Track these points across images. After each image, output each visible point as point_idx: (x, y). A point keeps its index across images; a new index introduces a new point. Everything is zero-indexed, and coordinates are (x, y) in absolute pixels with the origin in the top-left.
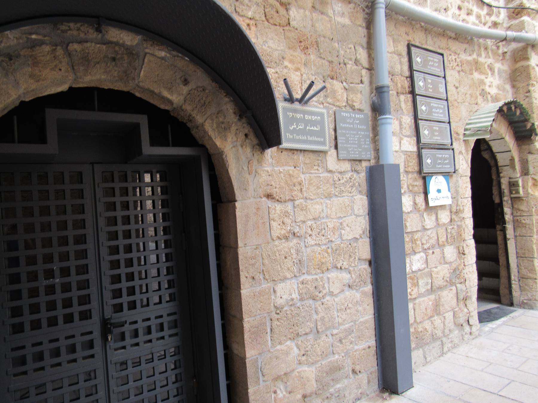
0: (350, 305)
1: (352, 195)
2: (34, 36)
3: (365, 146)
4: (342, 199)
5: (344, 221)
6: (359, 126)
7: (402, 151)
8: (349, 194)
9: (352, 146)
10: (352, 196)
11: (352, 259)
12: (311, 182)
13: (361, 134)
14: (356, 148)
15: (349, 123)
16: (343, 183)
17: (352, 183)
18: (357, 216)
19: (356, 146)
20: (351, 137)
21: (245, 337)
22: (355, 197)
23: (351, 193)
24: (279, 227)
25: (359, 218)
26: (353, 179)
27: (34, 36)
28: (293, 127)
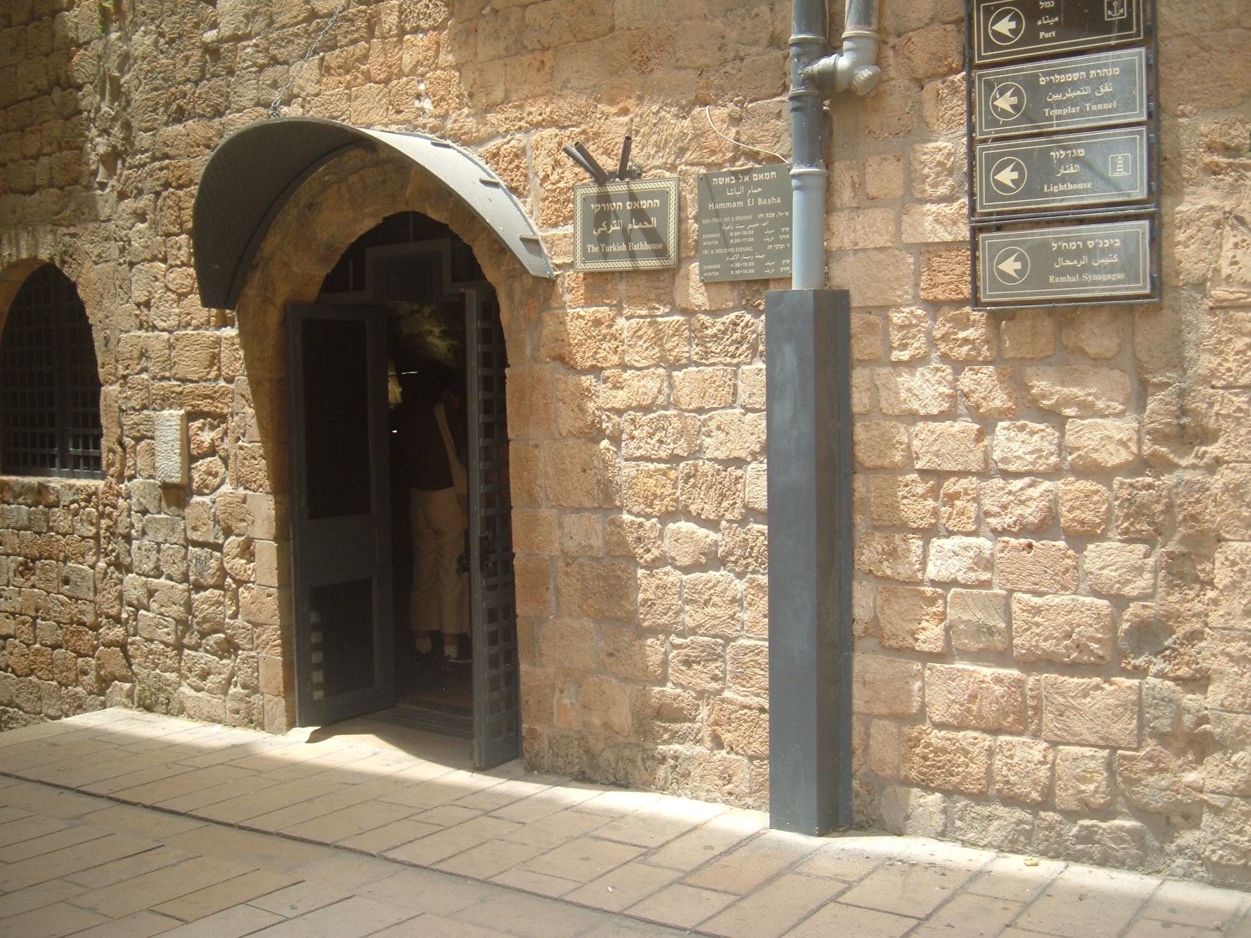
0: (715, 599)
1: (735, 361)
2: (326, 178)
3: (777, 247)
4: (710, 369)
5: (711, 418)
6: (760, 200)
7: (909, 247)
8: (728, 360)
9: (740, 249)
10: (738, 365)
11: (725, 504)
12: (640, 333)
13: (764, 220)
14: (748, 254)
15: (734, 199)
16: (715, 336)
17: (739, 334)
18: (748, 410)
19: (749, 249)
20: (736, 230)
21: (516, 581)
22: (744, 367)
23: (733, 356)
24: (571, 414)
25: (750, 416)
26: (743, 324)
27: (326, 178)
28: (599, 230)
